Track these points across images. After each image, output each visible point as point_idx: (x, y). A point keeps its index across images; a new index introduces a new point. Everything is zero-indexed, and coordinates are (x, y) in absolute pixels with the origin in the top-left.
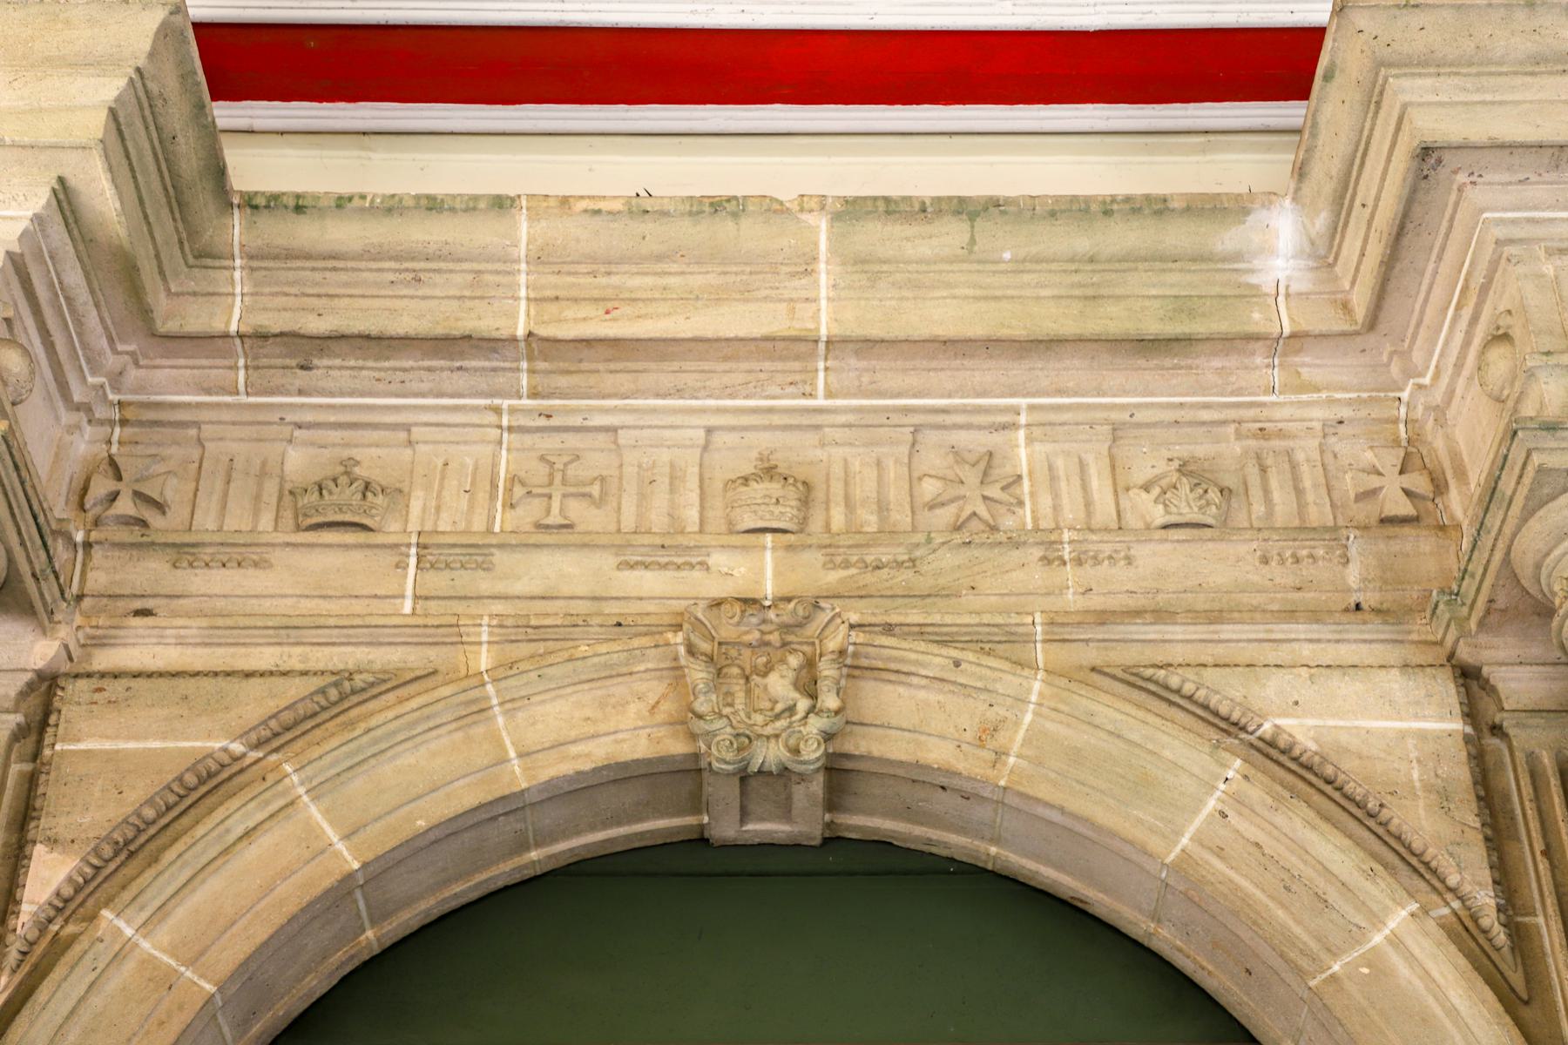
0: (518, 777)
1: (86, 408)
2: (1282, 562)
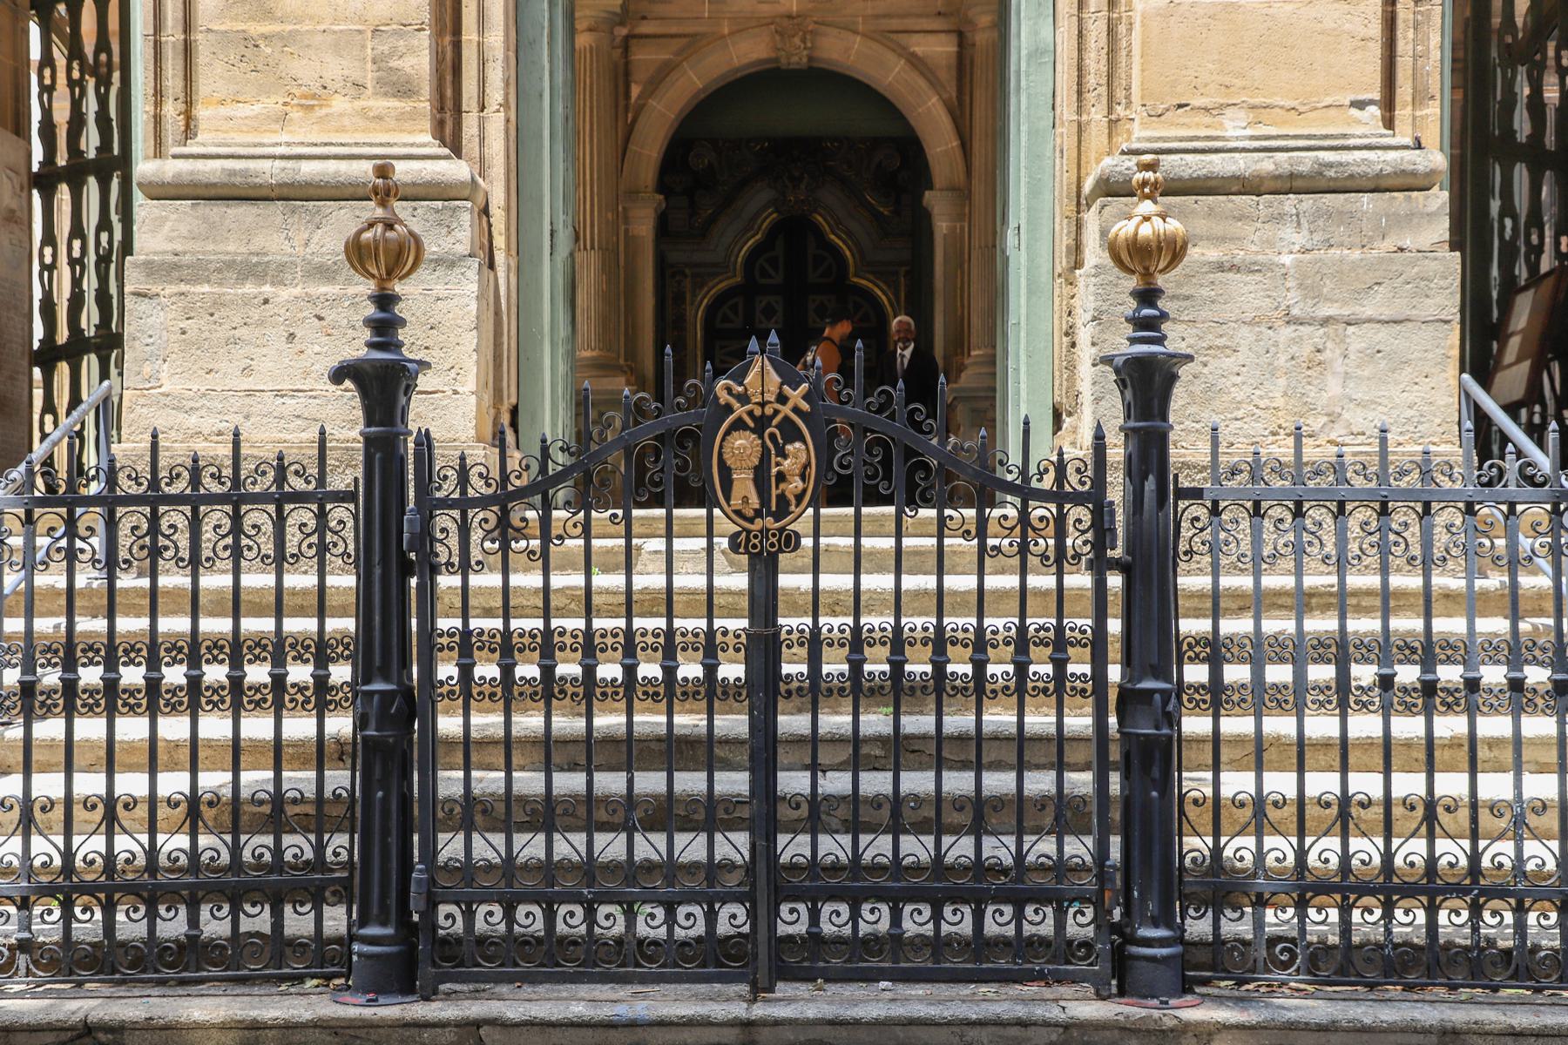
0: (736, 62)
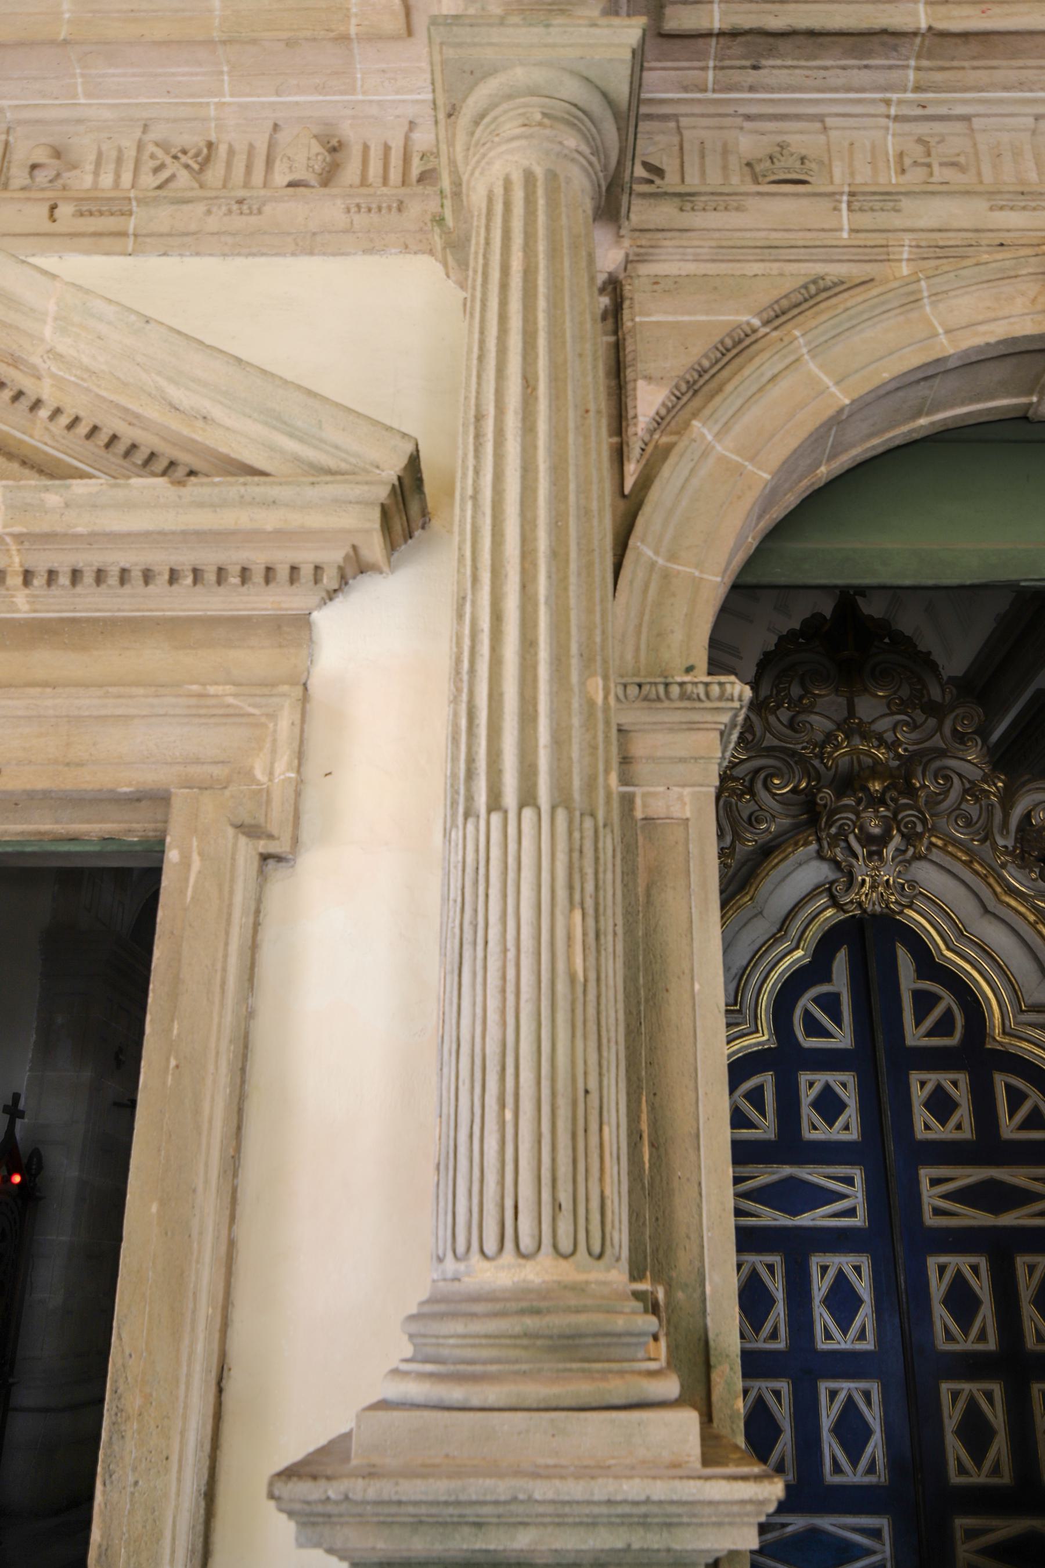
0: (947, 346)
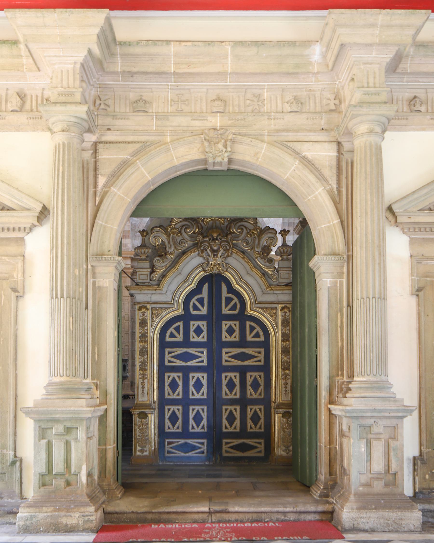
0: (176, 162)
1: (93, 85)
2: (310, 119)
